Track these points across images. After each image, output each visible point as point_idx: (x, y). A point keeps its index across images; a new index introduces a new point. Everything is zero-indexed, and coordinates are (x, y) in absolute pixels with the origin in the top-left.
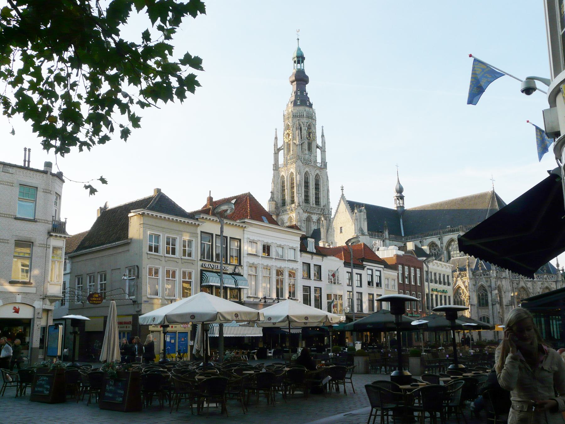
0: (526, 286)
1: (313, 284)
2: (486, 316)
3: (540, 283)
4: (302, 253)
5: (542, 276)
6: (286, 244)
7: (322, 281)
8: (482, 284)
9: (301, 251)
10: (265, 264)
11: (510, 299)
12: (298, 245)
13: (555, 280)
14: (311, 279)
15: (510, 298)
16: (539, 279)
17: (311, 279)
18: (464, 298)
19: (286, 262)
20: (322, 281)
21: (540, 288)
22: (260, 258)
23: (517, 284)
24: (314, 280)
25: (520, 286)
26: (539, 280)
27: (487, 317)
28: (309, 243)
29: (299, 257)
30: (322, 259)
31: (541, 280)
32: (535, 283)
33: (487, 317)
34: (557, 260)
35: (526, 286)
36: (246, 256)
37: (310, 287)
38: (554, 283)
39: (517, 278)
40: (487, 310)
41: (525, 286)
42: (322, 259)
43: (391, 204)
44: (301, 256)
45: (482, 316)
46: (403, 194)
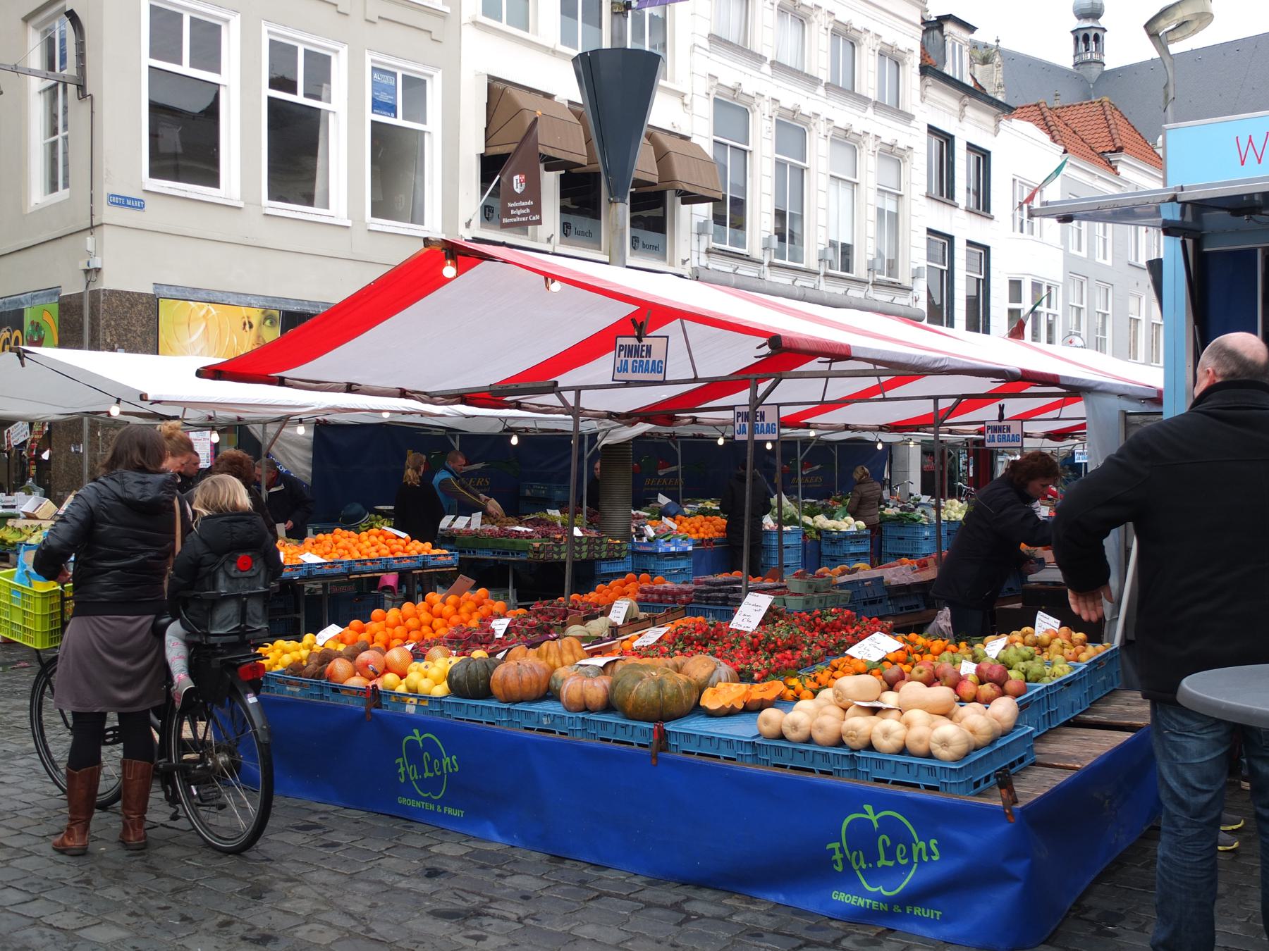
1: (962, 225)
4: (929, 80)
6: (874, 28)
7: (991, 218)
9: (925, 70)
10: (788, 103)
12: (910, 41)
14: (956, 206)
17: (956, 206)
19: (870, 110)
20: (991, 218)
22: (766, 68)
24: (968, 210)
28: (949, 46)
29: (917, 95)
30: (996, 126)
36: (705, 44)
37: (950, 239)
42: (996, 126)
43: (1062, 54)
44: (923, 98)
46: (1103, 22)
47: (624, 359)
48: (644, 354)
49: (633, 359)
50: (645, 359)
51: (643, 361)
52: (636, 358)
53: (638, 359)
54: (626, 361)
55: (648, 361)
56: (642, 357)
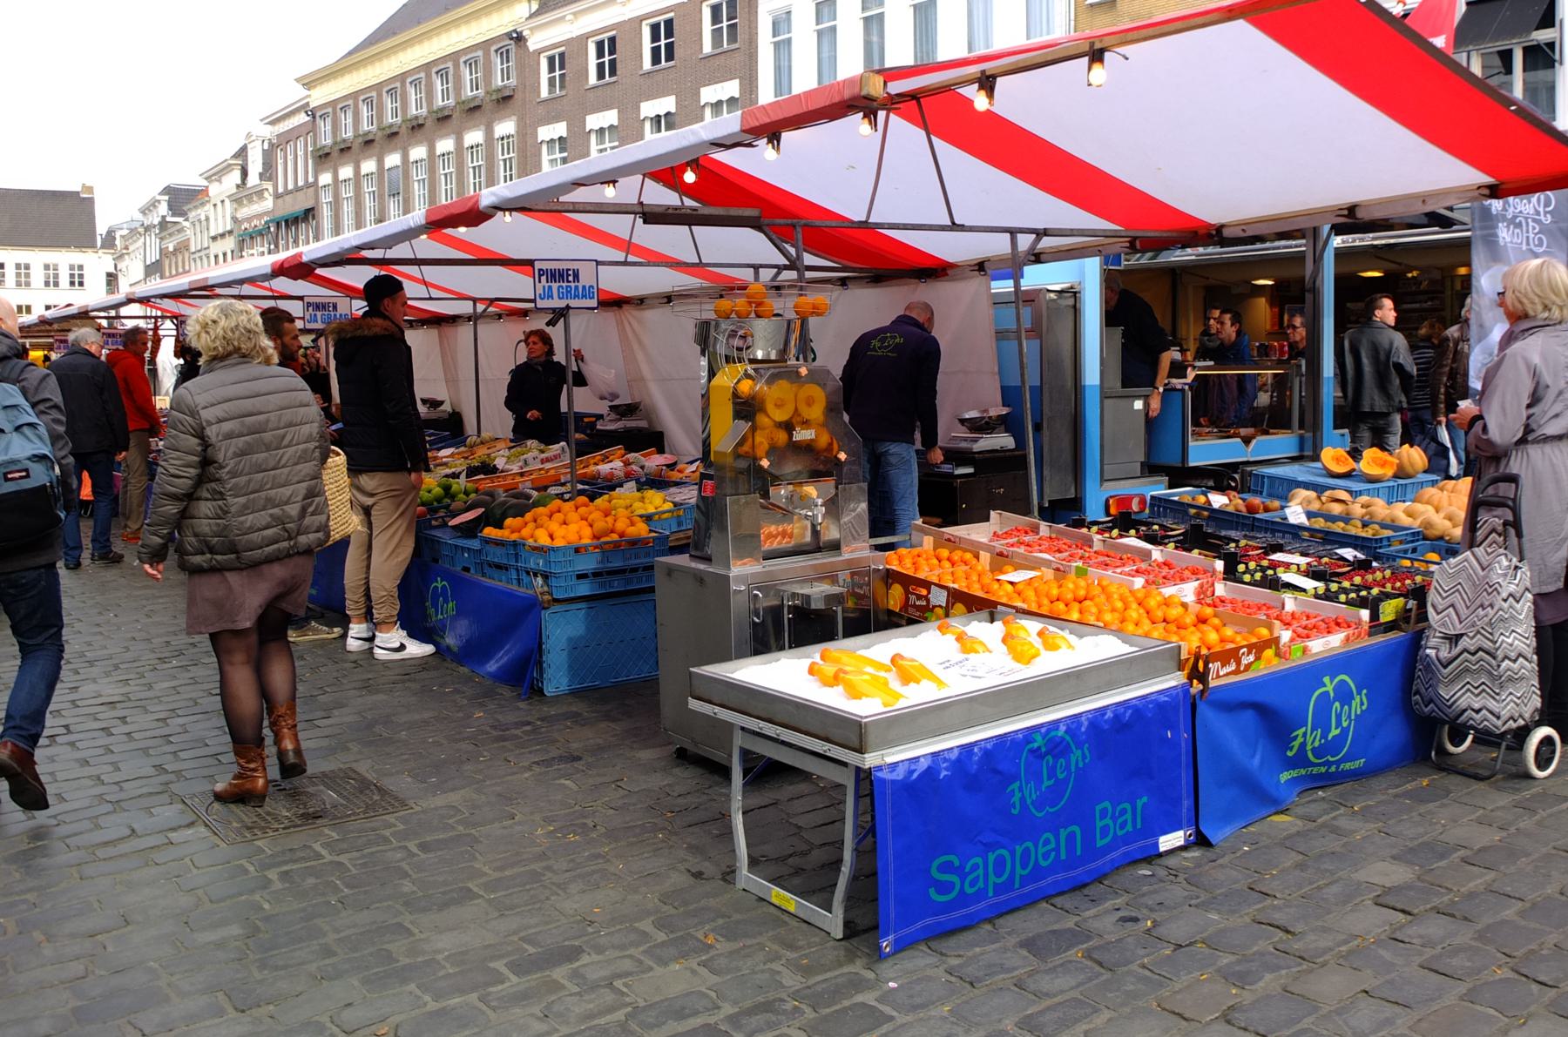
47: (547, 285)
48: (571, 278)
49: (558, 284)
50: (573, 285)
51: (570, 287)
52: (561, 284)
53: (564, 285)
54: (550, 287)
55: (577, 287)
56: (568, 281)
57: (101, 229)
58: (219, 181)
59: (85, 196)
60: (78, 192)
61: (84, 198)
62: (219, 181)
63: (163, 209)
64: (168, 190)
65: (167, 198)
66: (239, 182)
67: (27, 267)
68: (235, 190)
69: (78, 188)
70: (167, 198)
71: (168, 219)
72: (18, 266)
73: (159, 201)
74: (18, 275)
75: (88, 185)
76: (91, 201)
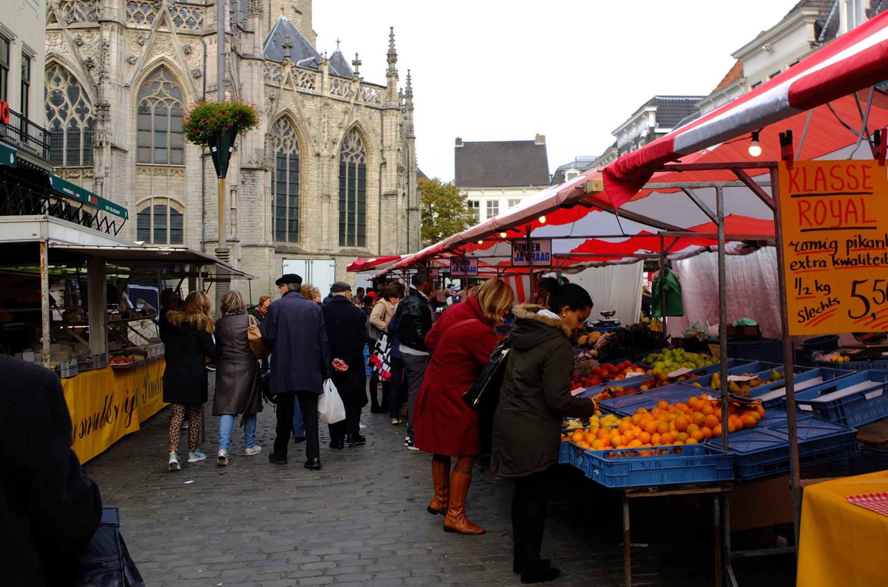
0: (299, 110)
2: (170, 205)
3: (339, 107)
5: (347, 85)
8: (162, 59)
11: (262, 146)
13: (380, 106)
15: (263, 139)
16: (339, 94)
18: (77, 116)
21: (340, 127)
23: (272, 100)
25: (281, 109)
26: (336, 96)
27: (172, 209)
31: (342, 98)
32: (327, 104)
33: (172, 209)
34: (392, 41)
35: (299, 110)
38: (376, 115)
39: (273, 76)
40: (176, 179)
41: (294, 110)
45: (152, 203)
57: (552, 171)
58: (770, 51)
59: (538, 144)
60: (533, 142)
61: (538, 146)
62: (770, 51)
63: (651, 121)
64: (654, 102)
65: (654, 109)
66: (813, 39)
67: (496, 203)
68: (809, 50)
69: (533, 138)
70: (654, 109)
71: (657, 130)
72: (489, 204)
73: (647, 113)
74: (489, 211)
75: (540, 134)
76: (543, 148)
